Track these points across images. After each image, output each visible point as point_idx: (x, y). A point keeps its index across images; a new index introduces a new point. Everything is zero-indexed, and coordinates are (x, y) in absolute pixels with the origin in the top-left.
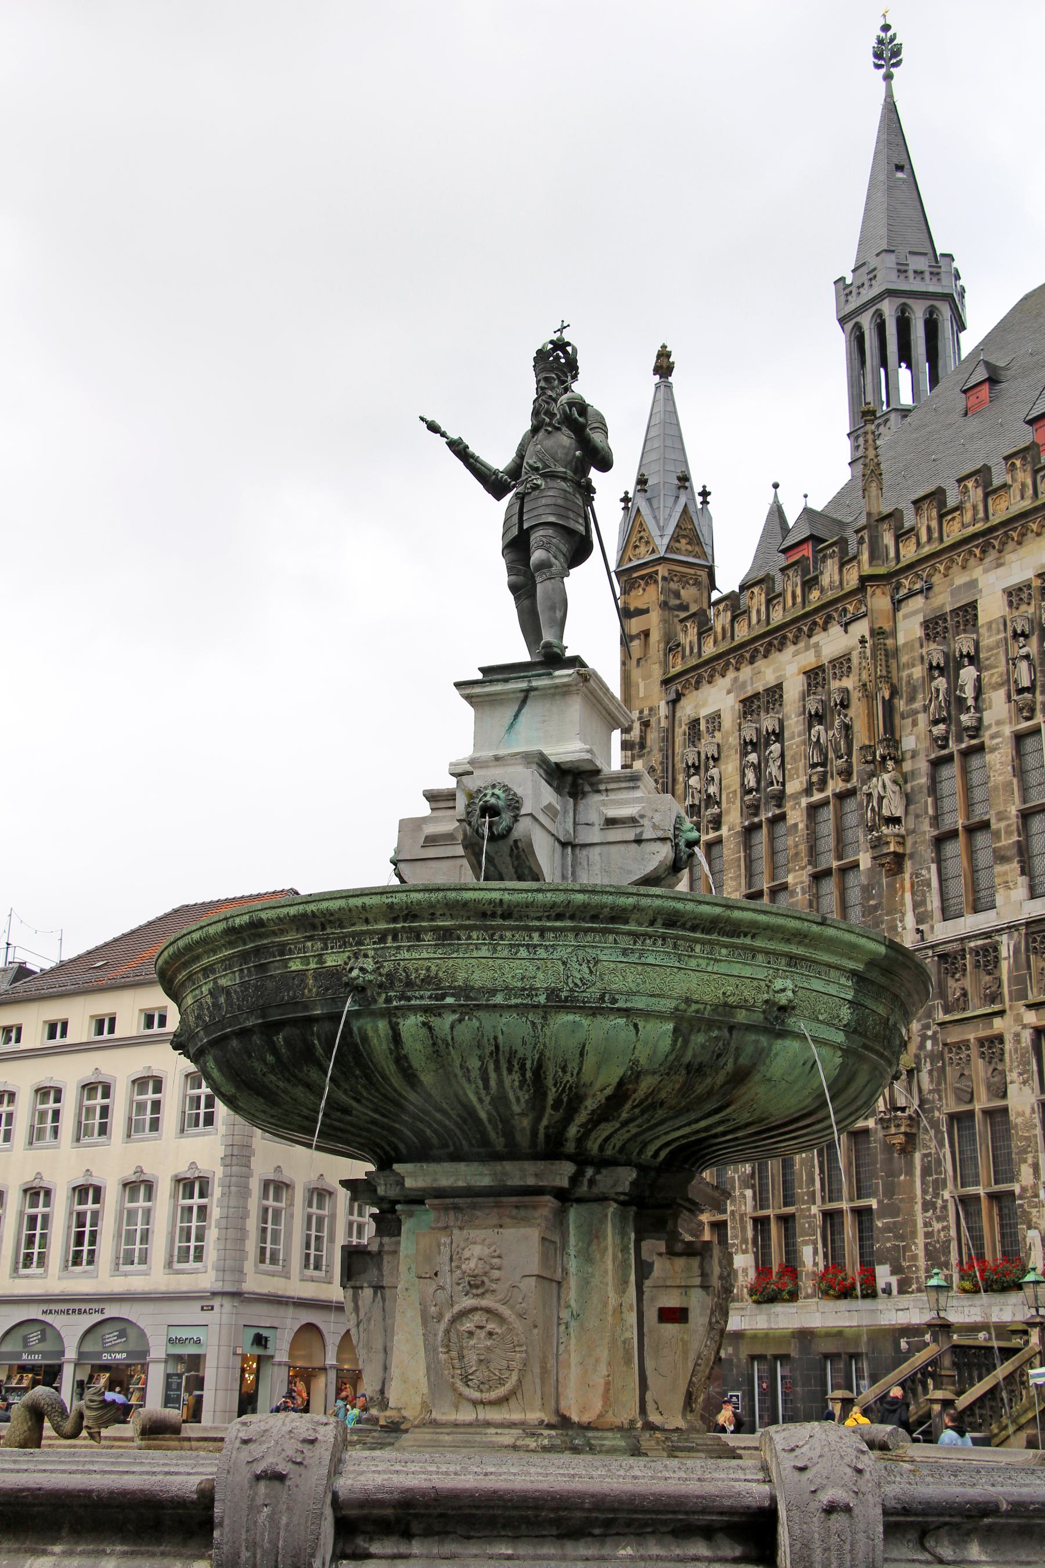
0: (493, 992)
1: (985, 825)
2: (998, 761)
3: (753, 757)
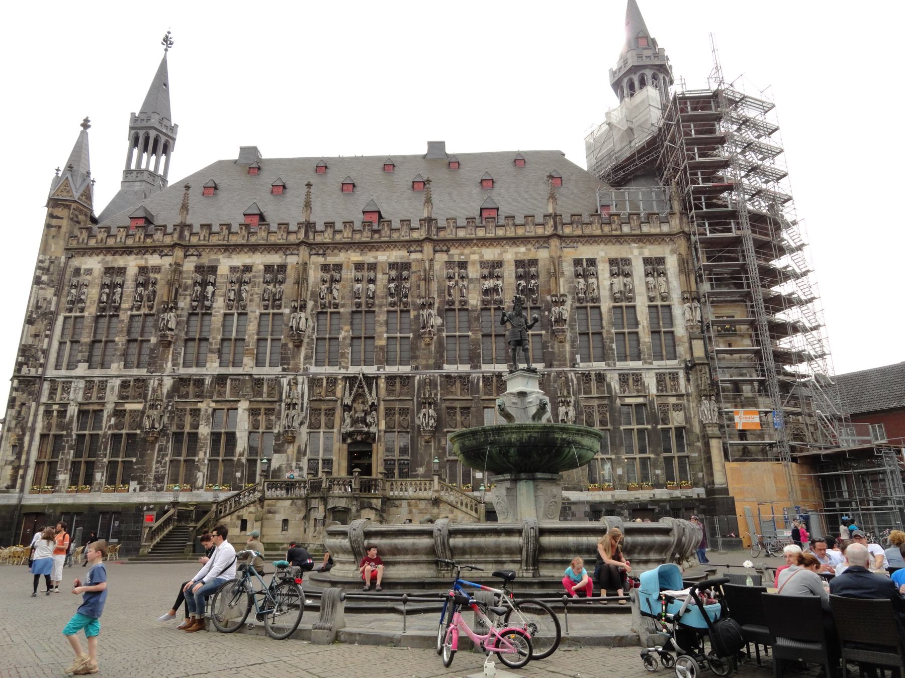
1: (207, 340)
2: (217, 319)
3: (107, 290)
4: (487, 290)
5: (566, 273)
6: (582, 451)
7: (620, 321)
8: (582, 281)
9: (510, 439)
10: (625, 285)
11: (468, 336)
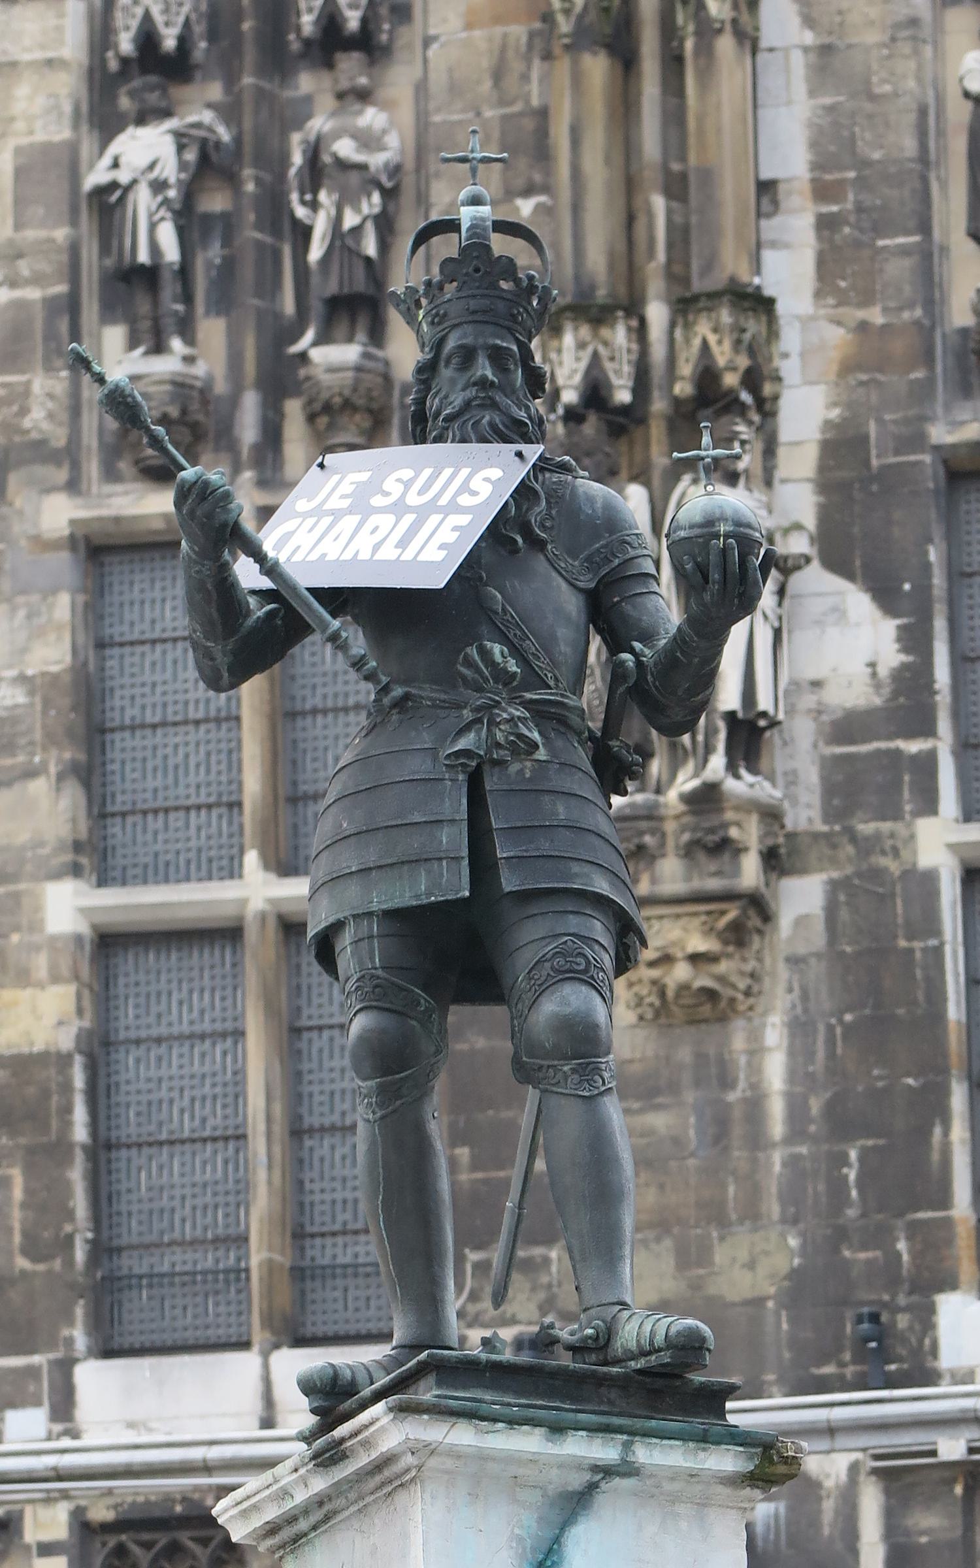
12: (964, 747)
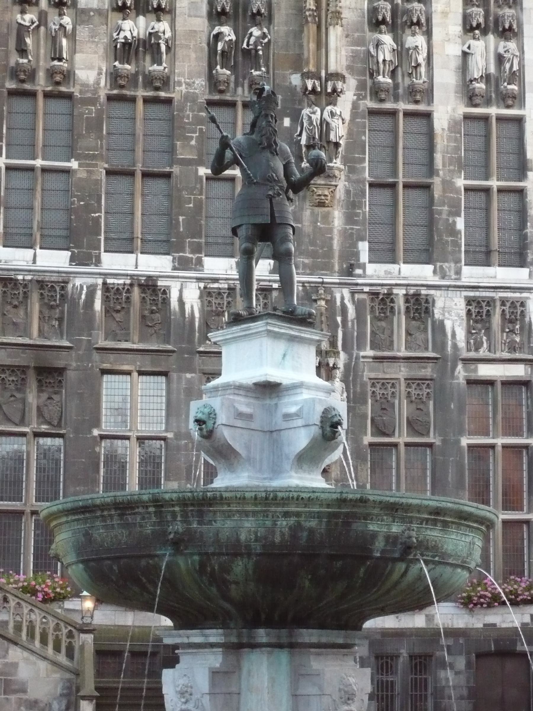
0: (450, 556)
4: (127, 44)
5: (346, 14)
6: (439, 569)
7: (478, 158)
8: (387, 39)
9: (236, 531)
10: (500, 59)
11: (67, 171)
12: (7, 145)
